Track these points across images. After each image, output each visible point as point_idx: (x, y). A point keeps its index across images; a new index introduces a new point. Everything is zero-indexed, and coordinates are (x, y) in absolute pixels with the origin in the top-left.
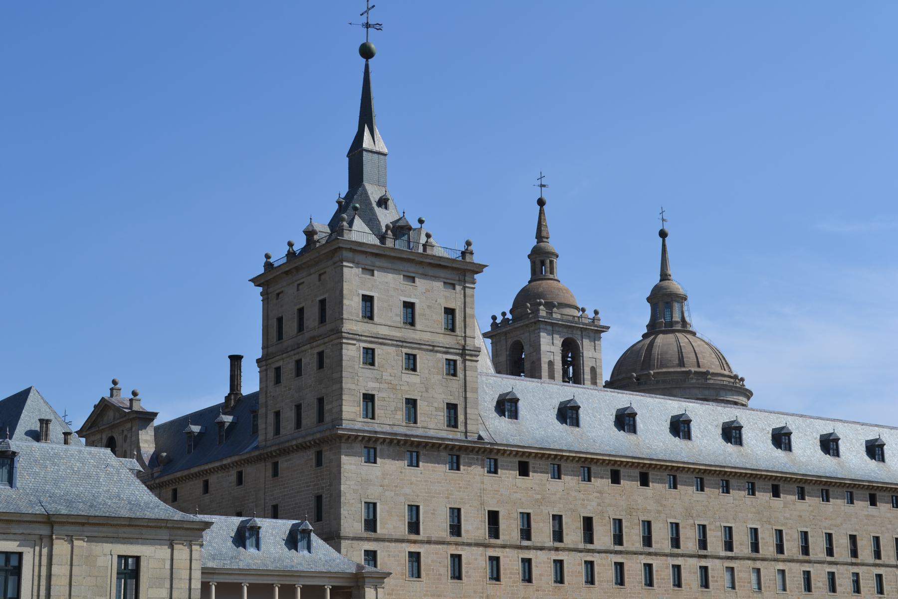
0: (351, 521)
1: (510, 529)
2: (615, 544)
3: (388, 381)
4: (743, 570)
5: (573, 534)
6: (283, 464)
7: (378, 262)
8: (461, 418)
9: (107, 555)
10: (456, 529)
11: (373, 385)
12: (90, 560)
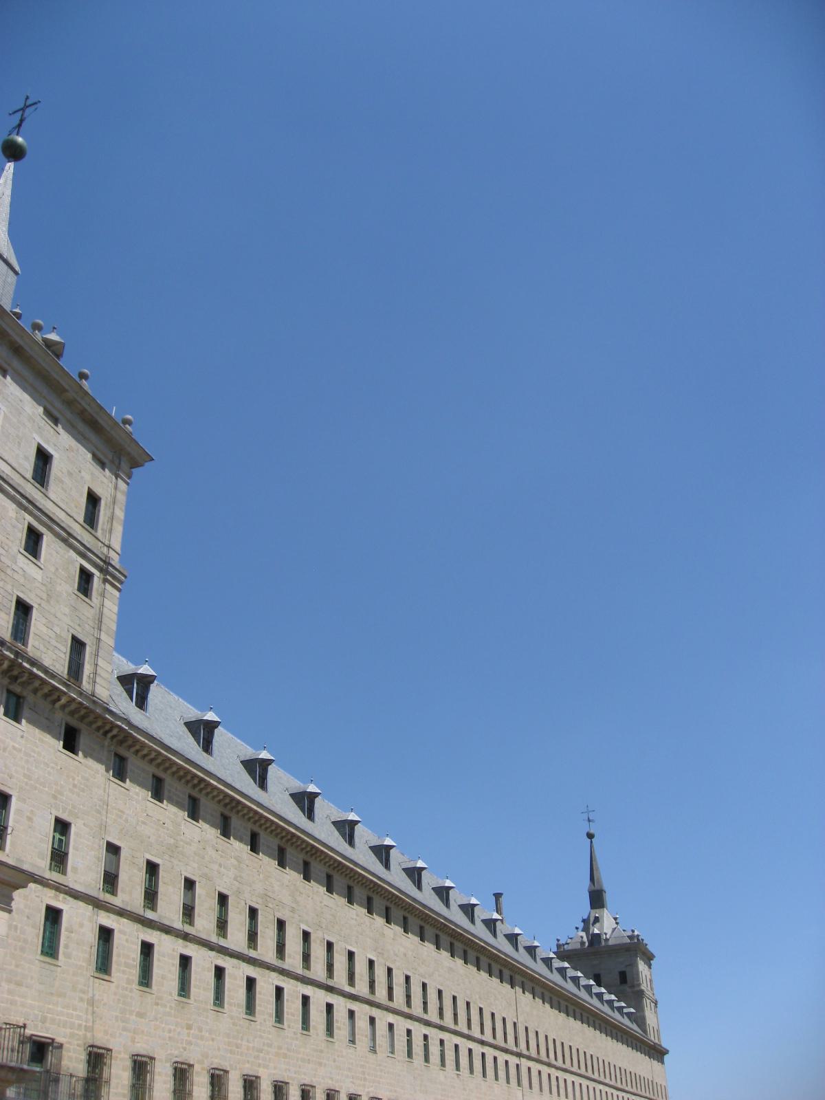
2: (249, 947)
7: (16, 363)
8: (88, 669)
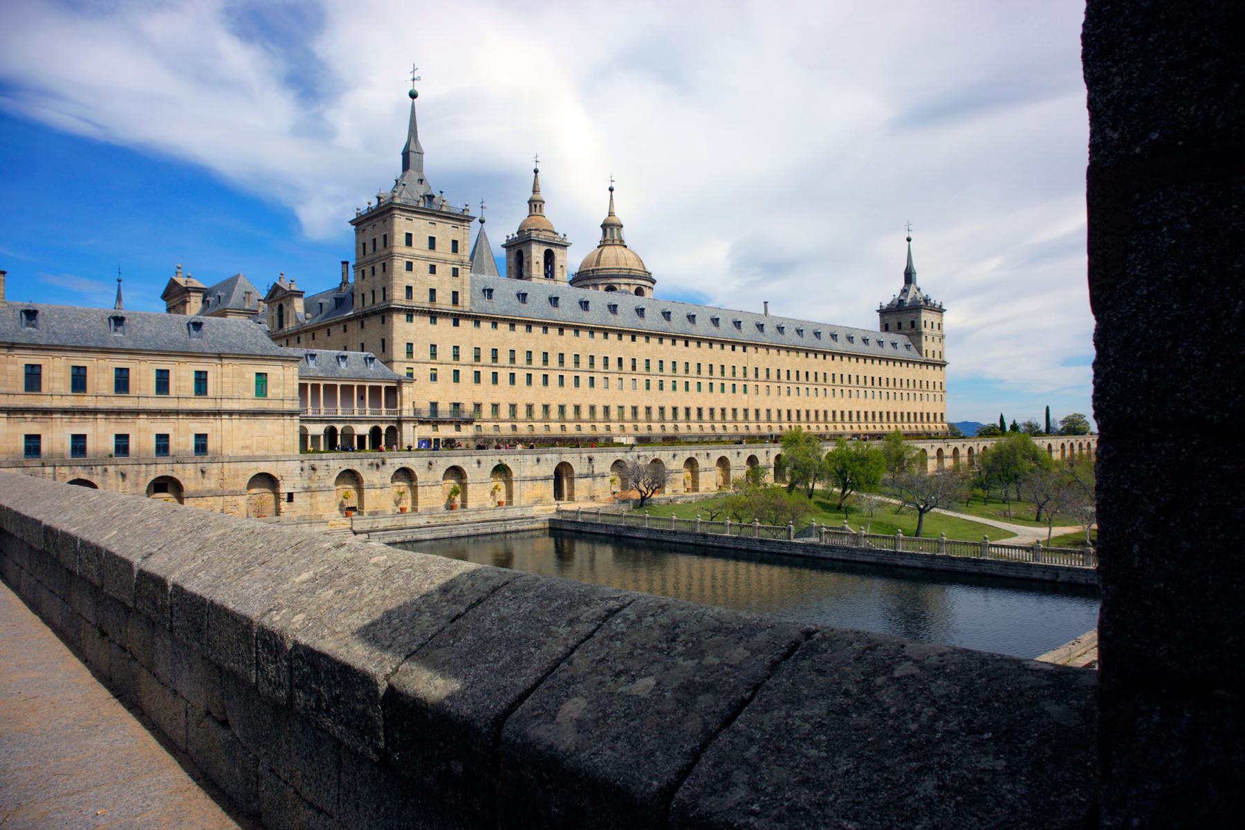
0: (399, 352)
1: (486, 357)
3: (421, 280)
4: (613, 379)
5: (521, 359)
6: (366, 323)
9: (250, 371)
10: (456, 356)
11: (412, 279)
12: (241, 375)
